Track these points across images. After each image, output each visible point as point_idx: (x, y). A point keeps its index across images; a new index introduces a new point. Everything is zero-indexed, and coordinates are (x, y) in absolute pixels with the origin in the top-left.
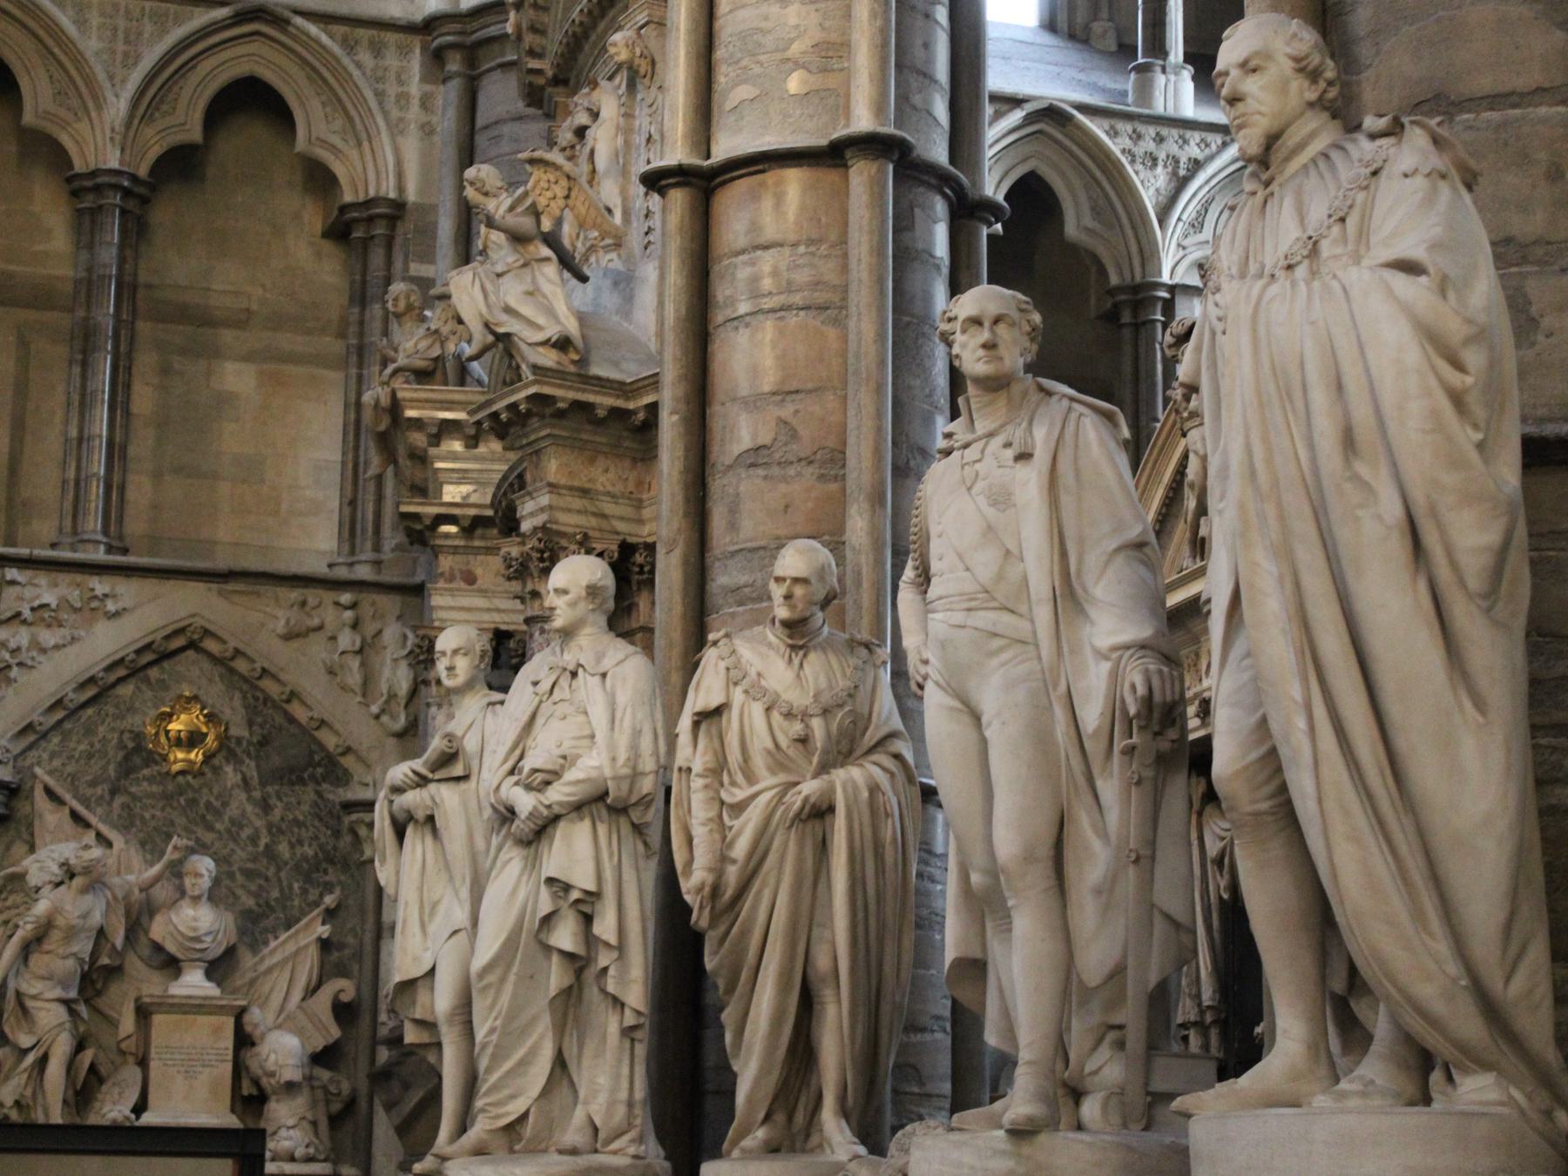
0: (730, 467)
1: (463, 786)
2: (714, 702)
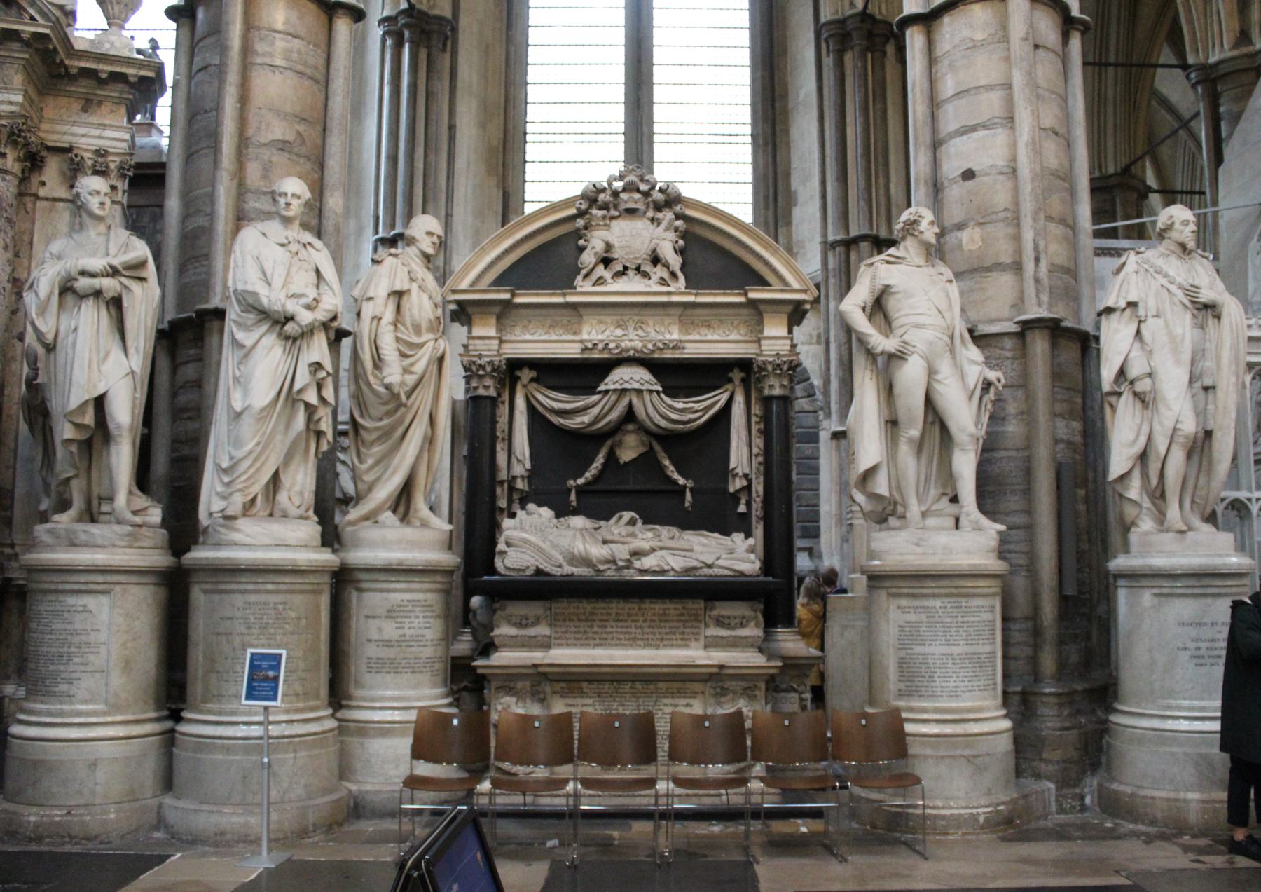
0: (265, 145)
1: (145, 284)
2: (405, 288)
